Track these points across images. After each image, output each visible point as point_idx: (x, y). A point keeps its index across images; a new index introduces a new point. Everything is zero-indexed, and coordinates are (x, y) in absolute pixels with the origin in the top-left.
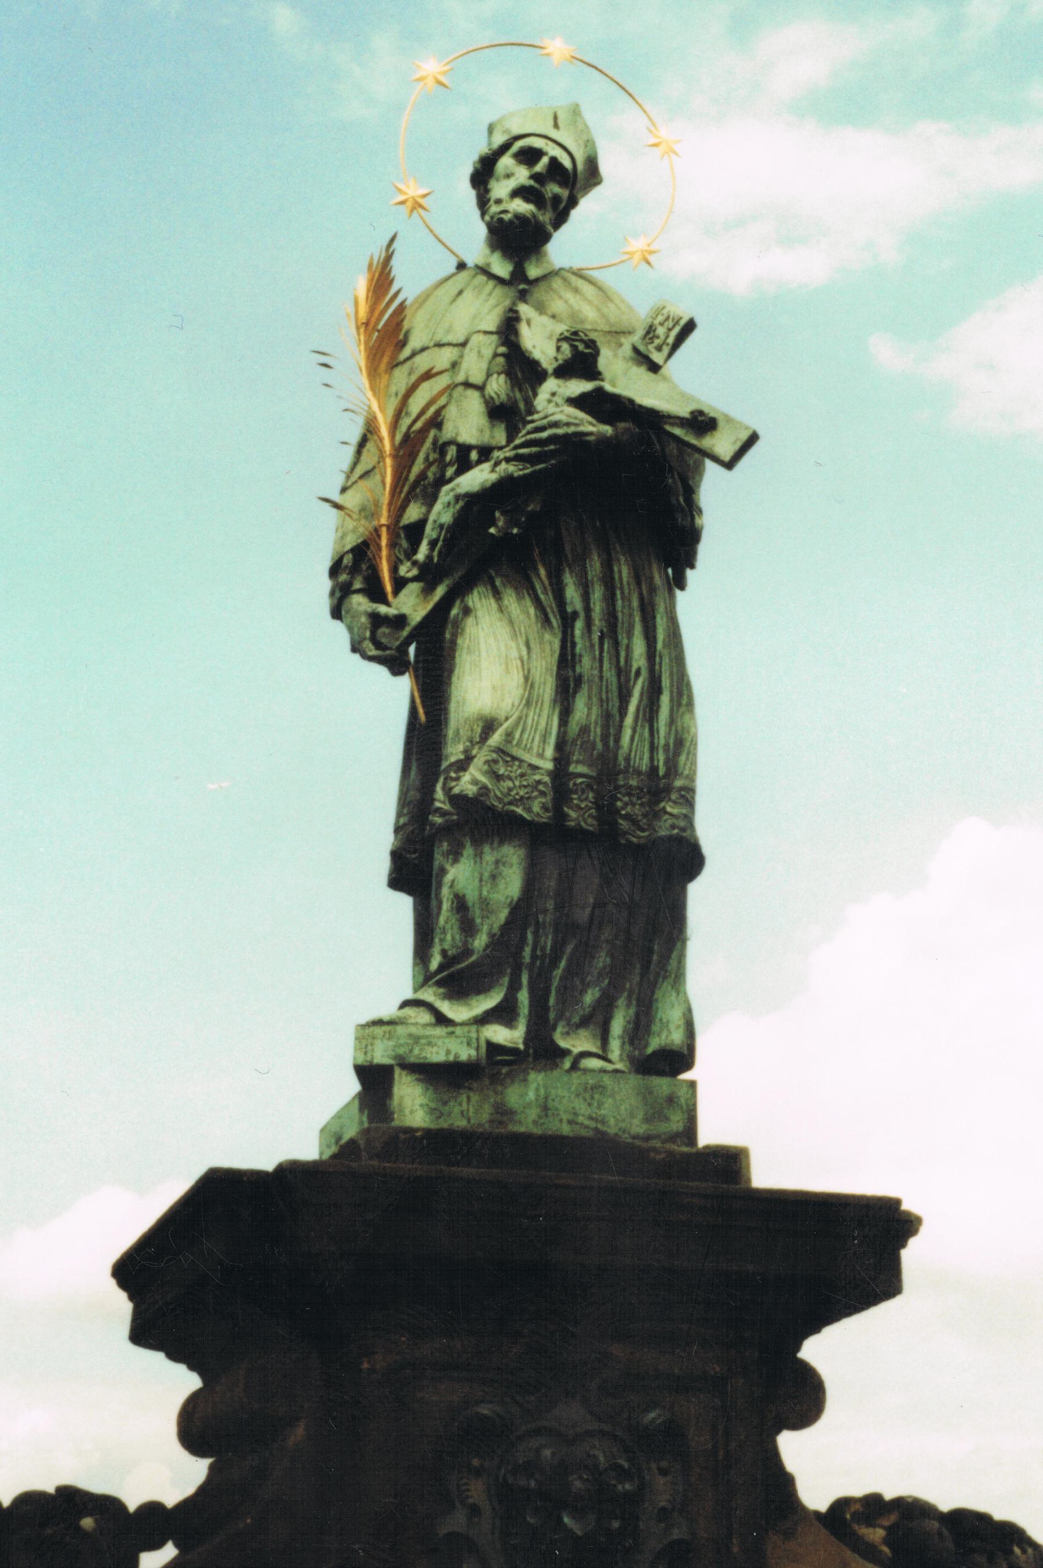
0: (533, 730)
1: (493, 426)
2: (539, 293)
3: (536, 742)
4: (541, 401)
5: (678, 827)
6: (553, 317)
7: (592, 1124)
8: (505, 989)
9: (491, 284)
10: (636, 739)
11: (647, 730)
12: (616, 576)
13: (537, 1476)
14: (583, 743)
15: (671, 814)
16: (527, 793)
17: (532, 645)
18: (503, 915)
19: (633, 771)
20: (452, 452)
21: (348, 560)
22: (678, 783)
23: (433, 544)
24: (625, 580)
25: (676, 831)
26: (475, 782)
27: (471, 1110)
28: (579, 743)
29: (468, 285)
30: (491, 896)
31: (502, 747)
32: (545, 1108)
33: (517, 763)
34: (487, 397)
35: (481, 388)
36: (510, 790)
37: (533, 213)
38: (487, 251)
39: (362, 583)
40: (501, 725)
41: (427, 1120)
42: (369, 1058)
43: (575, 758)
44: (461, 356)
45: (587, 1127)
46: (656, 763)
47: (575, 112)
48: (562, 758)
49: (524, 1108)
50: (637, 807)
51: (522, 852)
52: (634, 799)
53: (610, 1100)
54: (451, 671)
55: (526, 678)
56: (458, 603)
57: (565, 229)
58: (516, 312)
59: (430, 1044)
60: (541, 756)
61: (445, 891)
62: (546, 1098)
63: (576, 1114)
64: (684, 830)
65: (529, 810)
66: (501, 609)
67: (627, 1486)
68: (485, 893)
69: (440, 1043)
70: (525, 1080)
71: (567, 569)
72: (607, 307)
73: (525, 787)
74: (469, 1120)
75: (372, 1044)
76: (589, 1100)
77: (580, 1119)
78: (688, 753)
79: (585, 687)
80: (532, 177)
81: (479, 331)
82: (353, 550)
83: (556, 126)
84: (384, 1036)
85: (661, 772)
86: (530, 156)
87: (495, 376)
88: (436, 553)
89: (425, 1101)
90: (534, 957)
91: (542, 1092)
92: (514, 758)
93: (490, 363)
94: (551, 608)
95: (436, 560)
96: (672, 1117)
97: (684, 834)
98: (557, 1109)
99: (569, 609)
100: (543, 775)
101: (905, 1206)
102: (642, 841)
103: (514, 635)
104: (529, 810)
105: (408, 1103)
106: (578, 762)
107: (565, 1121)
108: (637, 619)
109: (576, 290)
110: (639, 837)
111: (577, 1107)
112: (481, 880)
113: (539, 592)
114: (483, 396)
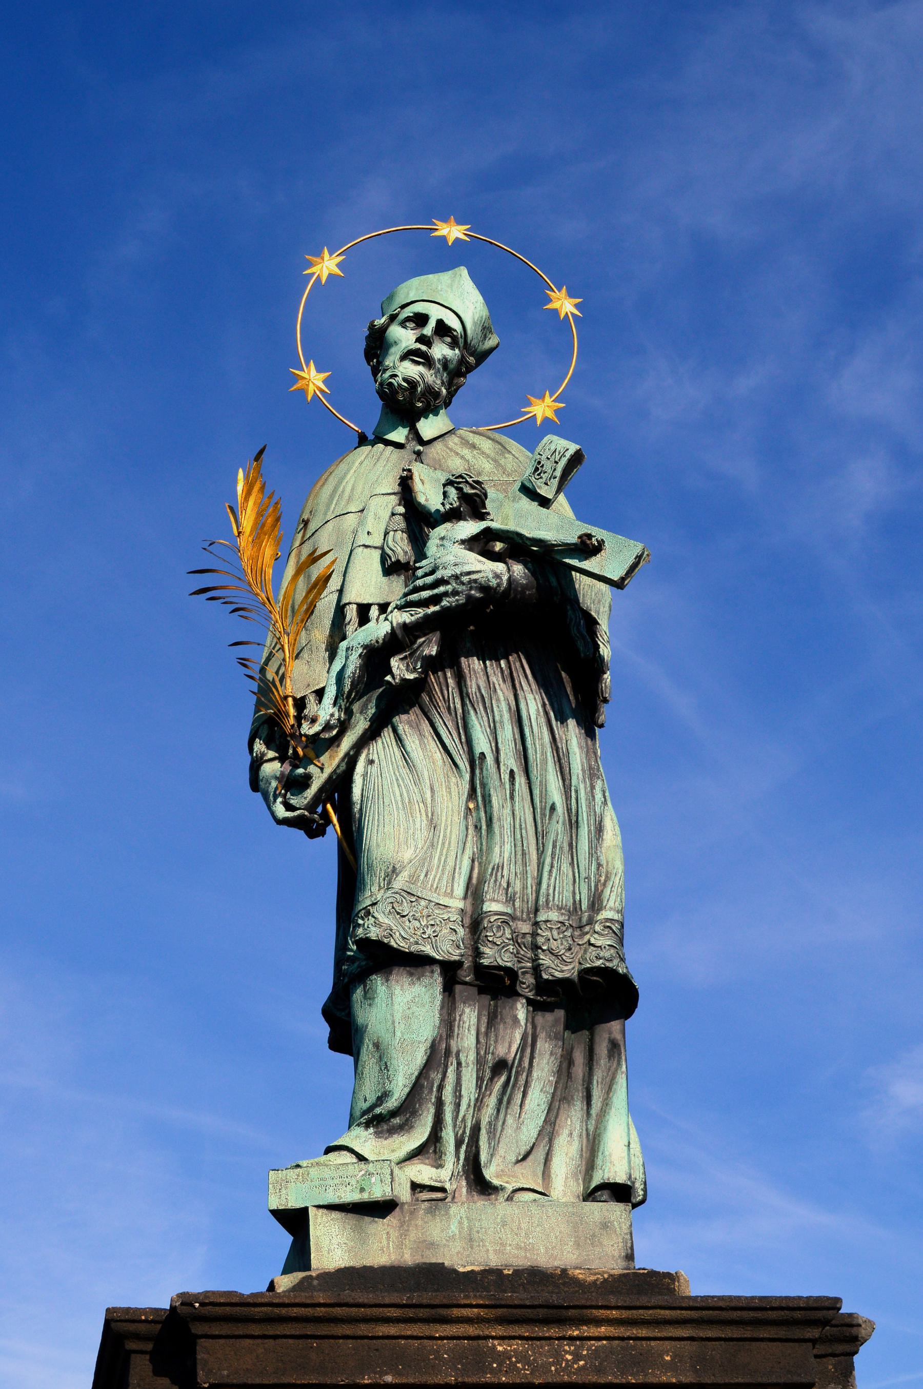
0: (440, 870)
2: (437, 449)
10: (554, 875)
14: (496, 881)
16: (434, 932)
19: (553, 905)
31: (405, 889)
33: (423, 903)
46: (578, 898)
49: (447, 1240)
50: (559, 941)
52: (555, 933)
60: (451, 895)
62: (470, 1229)
65: (435, 948)
68: (398, 1034)
70: (447, 1213)
71: (472, 712)
72: (505, 458)
85: (584, 906)
96: (605, 1243)
99: (477, 751)
105: (325, 1242)
106: (493, 900)
107: (491, 1252)
108: (549, 754)
109: (473, 446)
110: (562, 971)
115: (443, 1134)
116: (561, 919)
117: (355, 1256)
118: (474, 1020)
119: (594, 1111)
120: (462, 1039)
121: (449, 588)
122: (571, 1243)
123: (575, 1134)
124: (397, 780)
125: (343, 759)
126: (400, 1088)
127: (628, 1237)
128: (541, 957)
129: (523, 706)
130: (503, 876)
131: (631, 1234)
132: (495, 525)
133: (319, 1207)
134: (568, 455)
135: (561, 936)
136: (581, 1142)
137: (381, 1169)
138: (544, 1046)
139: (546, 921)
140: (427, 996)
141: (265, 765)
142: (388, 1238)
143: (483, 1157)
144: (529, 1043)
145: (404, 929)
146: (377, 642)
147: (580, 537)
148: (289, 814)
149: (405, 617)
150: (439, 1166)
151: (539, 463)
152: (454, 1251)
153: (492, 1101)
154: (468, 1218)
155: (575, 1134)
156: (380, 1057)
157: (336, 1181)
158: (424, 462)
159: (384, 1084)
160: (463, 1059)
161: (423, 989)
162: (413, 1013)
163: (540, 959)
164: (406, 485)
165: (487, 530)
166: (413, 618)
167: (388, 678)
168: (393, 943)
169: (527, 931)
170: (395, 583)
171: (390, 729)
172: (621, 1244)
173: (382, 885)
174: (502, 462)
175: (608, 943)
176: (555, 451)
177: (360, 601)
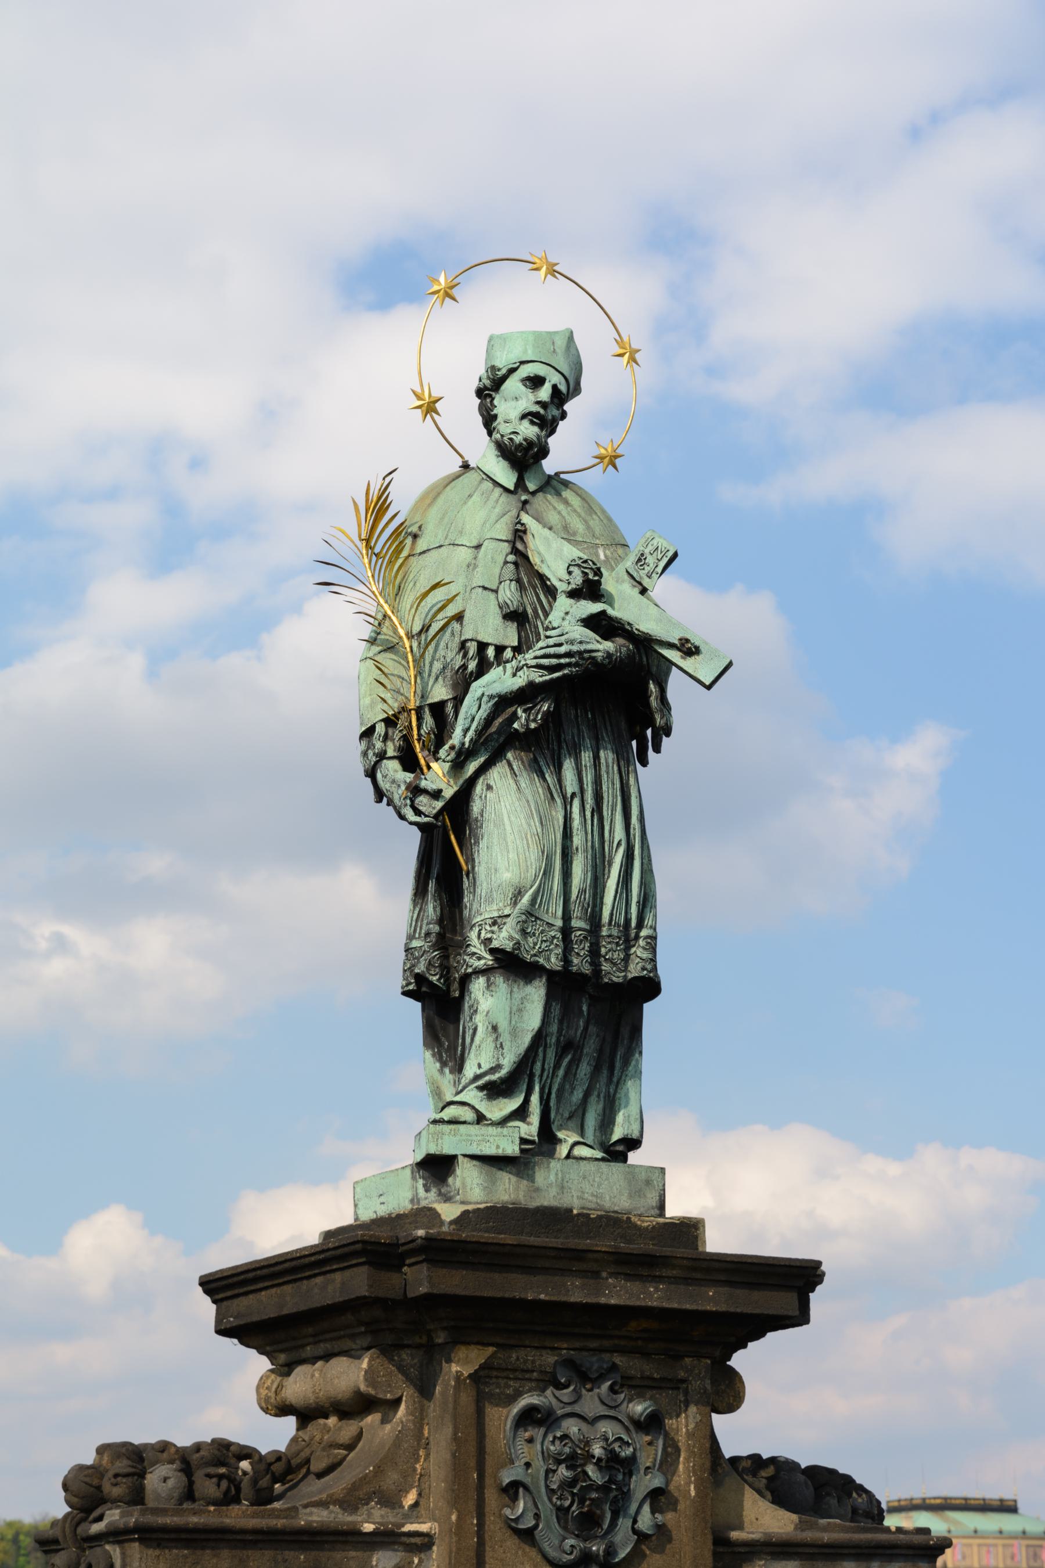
6: (550, 529)
7: (595, 1200)
8: (524, 1094)
9: (498, 490)
10: (617, 899)
12: (603, 761)
16: (546, 947)
18: (526, 1040)
20: (472, 648)
21: (380, 729)
24: (611, 765)
29: (477, 489)
30: (518, 1025)
31: (529, 910)
32: (563, 1188)
33: (538, 922)
34: (501, 600)
35: (496, 591)
37: (538, 435)
39: (395, 750)
40: (527, 892)
41: (482, 1195)
42: (440, 1148)
45: (590, 1202)
48: (567, 917)
51: (542, 992)
52: (614, 946)
53: (606, 1183)
55: (543, 852)
58: (523, 524)
60: (555, 916)
61: (479, 1020)
62: (563, 1180)
63: (583, 1192)
68: (513, 1023)
69: (491, 1140)
70: (548, 1167)
71: (567, 756)
73: (545, 941)
74: (510, 1195)
75: (442, 1139)
76: (592, 1183)
82: (384, 720)
84: (450, 1133)
85: (634, 923)
87: (508, 582)
88: (467, 740)
89: (480, 1182)
90: (543, 1070)
91: (560, 1175)
92: (537, 918)
93: (502, 567)
94: (557, 790)
95: (467, 746)
98: (570, 1188)
99: (569, 791)
100: (556, 931)
104: (548, 960)
105: (469, 1181)
107: (575, 1197)
109: (566, 502)
110: (618, 977)
111: (583, 1186)
112: (511, 1013)
116: (619, 935)
117: (488, 1194)
118: (557, 1012)
119: (615, 1079)
120: (549, 1026)
121: (573, 660)
122: (626, 1194)
123: (602, 1095)
126: (508, 1063)
127: (662, 1192)
128: (604, 964)
130: (585, 899)
131: (664, 1190)
132: (610, 612)
133: (465, 1156)
134: (670, 554)
135: (619, 948)
136: (605, 1101)
137: (513, 1133)
138: (593, 1029)
139: (609, 936)
140: (536, 996)
141: (385, 761)
142: (510, 1182)
144: (586, 1029)
145: (527, 943)
146: (511, 694)
147: (680, 640)
148: (418, 819)
150: (529, 1124)
151: (642, 555)
152: (552, 1195)
153: (561, 1072)
154: (561, 1171)
155: (602, 1095)
156: (497, 1038)
157: (479, 1138)
158: (529, 513)
159: (498, 1059)
160: (548, 1041)
161: (534, 989)
165: (603, 613)
166: (541, 679)
168: (521, 956)
169: (594, 941)
170: (509, 628)
171: (505, 761)
172: (658, 1198)
173: (509, 903)
174: (591, 523)
175: (650, 957)
177: (480, 638)
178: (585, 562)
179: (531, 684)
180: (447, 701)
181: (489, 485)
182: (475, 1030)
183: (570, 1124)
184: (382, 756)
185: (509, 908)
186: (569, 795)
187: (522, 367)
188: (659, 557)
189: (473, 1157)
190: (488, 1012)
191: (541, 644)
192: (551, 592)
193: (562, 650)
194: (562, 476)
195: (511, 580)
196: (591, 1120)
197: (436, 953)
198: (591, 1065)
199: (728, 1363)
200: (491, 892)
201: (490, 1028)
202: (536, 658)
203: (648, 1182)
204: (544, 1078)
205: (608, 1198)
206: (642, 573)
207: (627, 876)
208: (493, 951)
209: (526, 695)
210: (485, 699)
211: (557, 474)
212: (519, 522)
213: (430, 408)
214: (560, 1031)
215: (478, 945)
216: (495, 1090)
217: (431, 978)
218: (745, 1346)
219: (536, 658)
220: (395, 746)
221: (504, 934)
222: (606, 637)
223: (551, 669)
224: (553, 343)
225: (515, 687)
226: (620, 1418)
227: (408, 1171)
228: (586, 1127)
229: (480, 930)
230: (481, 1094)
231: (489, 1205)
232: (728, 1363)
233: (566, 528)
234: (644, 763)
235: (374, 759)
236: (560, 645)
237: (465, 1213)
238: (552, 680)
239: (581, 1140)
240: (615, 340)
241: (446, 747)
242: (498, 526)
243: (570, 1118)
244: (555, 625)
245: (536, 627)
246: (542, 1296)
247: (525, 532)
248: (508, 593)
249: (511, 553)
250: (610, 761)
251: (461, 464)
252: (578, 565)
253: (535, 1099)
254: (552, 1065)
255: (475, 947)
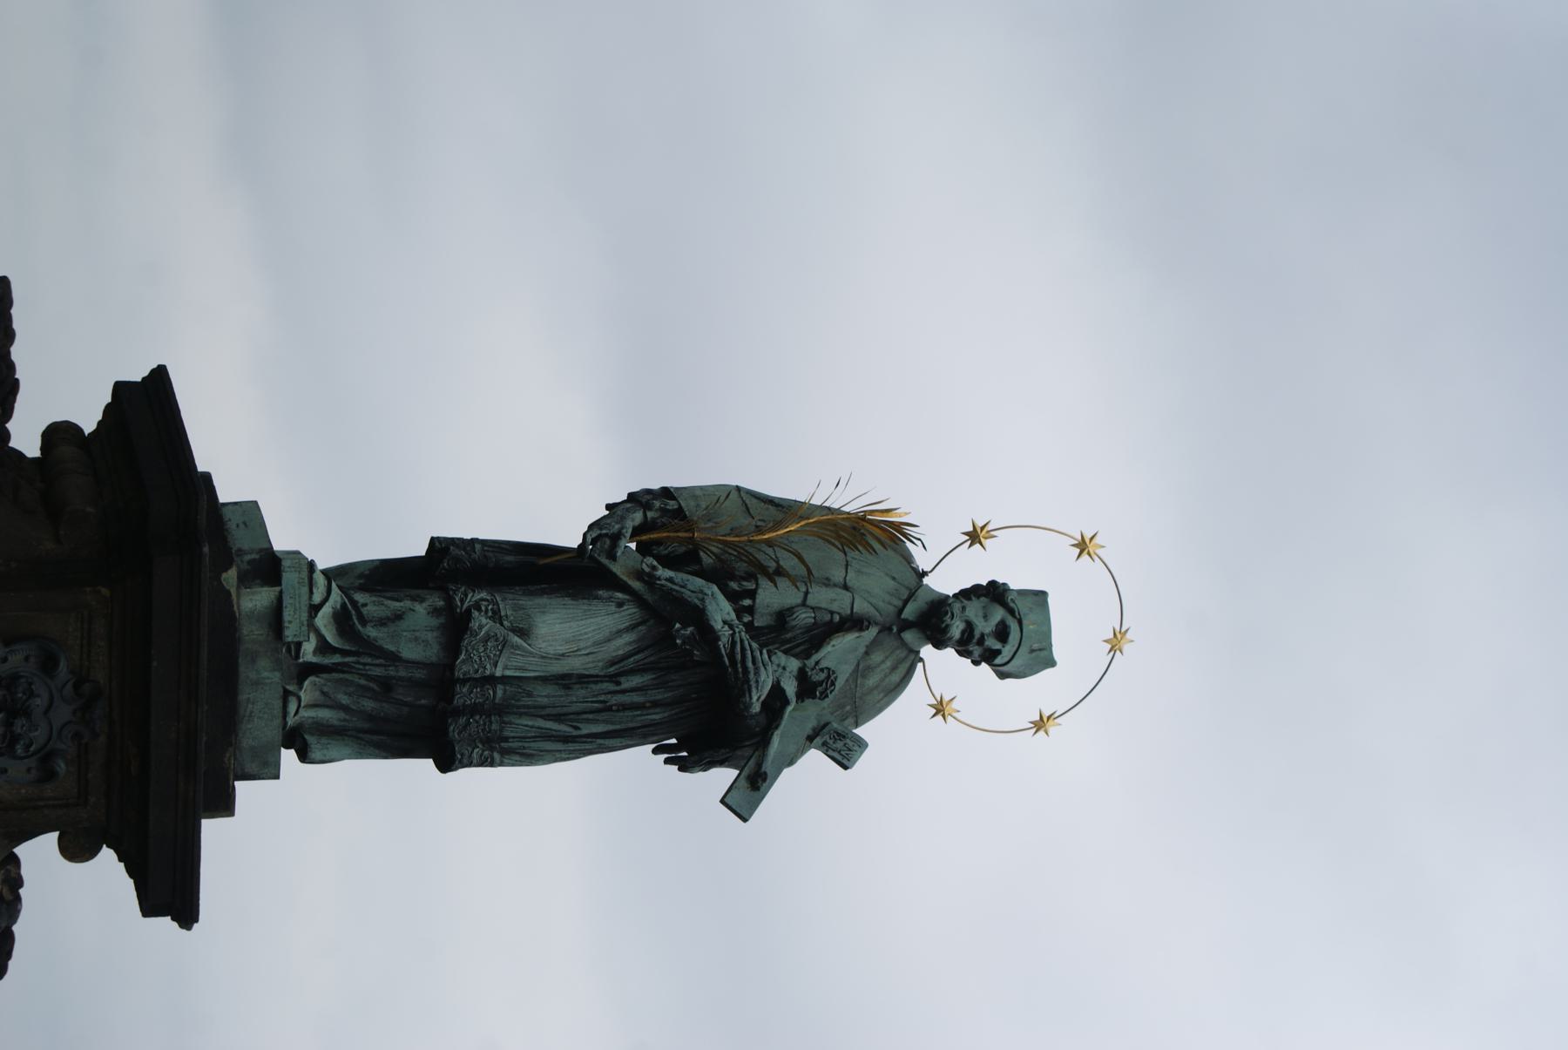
1: (771, 615)
3: (515, 664)
4: (781, 658)
5: (462, 758)
6: (867, 653)
8: (340, 647)
9: (899, 603)
11: (533, 734)
13: (25, 697)
14: (520, 693)
15: (472, 752)
17: (590, 656)
18: (391, 648)
20: (750, 585)
21: (672, 505)
22: (496, 755)
23: (670, 580)
24: (649, 717)
25: (459, 756)
26: (481, 627)
27: (255, 637)
28: (520, 690)
30: (403, 638)
33: (498, 653)
35: (804, 604)
36: (477, 651)
38: (930, 598)
42: (287, 569)
43: (507, 688)
44: (835, 585)
45: (245, 711)
46: (510, 740)
47: (1051, 663)
48: (504, 680)
51: (434, 659)
54: (574, 597)
55: (563, 655)
56: (627, 597)
57: (955, 653)
58: (868, 628)
59: (295, 609)
60: (506, 668)
61: (407, 603)
63: (253, 703)
64: (460, 762)
65: (463, 661)
66: (619, 632)
67: (19, 751)
68: (405, 634)
70: (274, 670)
71: (654, 676)
74: (248, 635)
77: (250, 706)
78: (520, 761)
79: (562, 692)
80: (982, 635)
81: (854, 599)
83: (1032, 651)
86: (1002, 633)
87: (813, 615)
88: (663, 582)
90: (365, 664)
91: (267, 681)
92: (501, 651)
93: (826, 609)
94: (623, 667)
95: (658, 582)
97: (457, 762)
98: (256, 691)
99: (622, 679)
101: (195, 925)
102: (451, 734)
103: (596, 644)
105: (258, 597)
106: (505, 691)
109: (894, 668)
110: (453, 731)
112: (414, 631)
113: (636, 657)
114: (798, 606)
115: (338, 655)
117: (247, 615)
118: (418, 675)
119: (361, 735)
123: (346, 724)
124: (600, 629)
125: (625, 583)
126: (371, 632)
129: (657, 710)
132: (790, 708)
133: (281, 592)
134: (845, 762)
138: (406, 710)
139: (491, 722)
143: (325, 676)
144: (406, 704)
147: (765, 773)
149: (724, 642)
150: (315, 653)
151: (844, 737)
153: (363, 682)
155: (346, 724)
157: (297, 605)
160: (391, 668)
161: (436, 651)
162: (419, 644)
163: (464, 716)
164: (854, 623)
166: (722, 646)
167: (678, 625)
174: (875, 692)
176: (850, 750)
178: (833, 684)
179: (718, 639)
180: (701, 565)
181: (905, 595)
182: (397, 600)
183: (318, 693)
184: (646, 507)
185: (509, 625)
186: (618, 679)
187: (1016, 621)
188: (842, 752)
189: (280, 599)
190: (413, 611)
191: (755, 645)
192: (807, 655)
193: (750, 664)
194: (920, 665)
195: (815, 618)
196: (325, 714)
197: (468, 563)
198: (372, 711)
199: (105, 846)
200: (523, 609)
201: (399, 613)
202: (742, 641)
203: (266, 764)
204: (357, 666)
205: (250, 726)
206: (828, 736)
207: (550, 737)
208: (468, 611)
209: (707, 634)
210: (700, 596)
211: (921, 660)
212: (870, 623)
213: (974, 537)
214: (401, 679)
215: (474, 599)
216: (342, 619)
217: (446, 561)
218: (120, 860)
219: (742, 641)
220: (657, 518)
221: (484, 621)
222: (765, 705)
223: (732, 655)
224: (1040, 650)
225: (713, 623)
226: (51, 743)
227: (266, 546)
228: (317, 709)
229: (487, 600)
230: (339, 607)
231: (237, 614)
232: (105, 846)
233: (869, 669)
234: (655, 751)
235: (644, 500)
236: (754, 662)
237: (228, 593)
238: (723, 657)
239: (302, 704)
240: (1055, 712)
241: (655, 563)
242: (866, 604)
243: (323, 693)
244: (773, 658)
245: (773, 643)
246: (155, 664)
247: (861, 630)
248: (804, 616)
249: (840, 618)
250: (654, 717)
251: (925, 570)
252: (829, 677)
253: (337, 659)
254: (369, 673)
255: (473, 596)
